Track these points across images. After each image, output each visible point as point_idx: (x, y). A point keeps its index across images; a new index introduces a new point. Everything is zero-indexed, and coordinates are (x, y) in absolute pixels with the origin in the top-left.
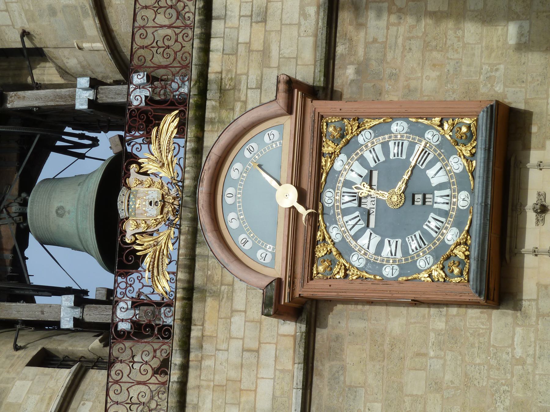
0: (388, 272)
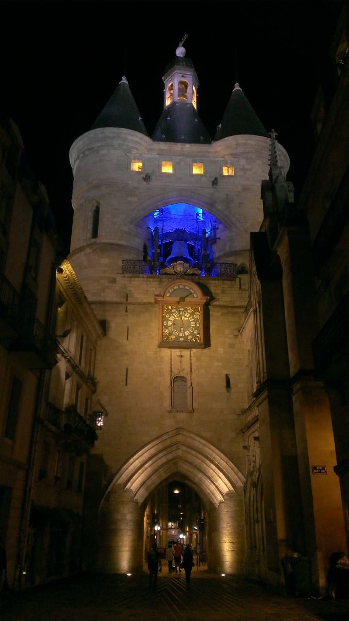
0: (165, 323)
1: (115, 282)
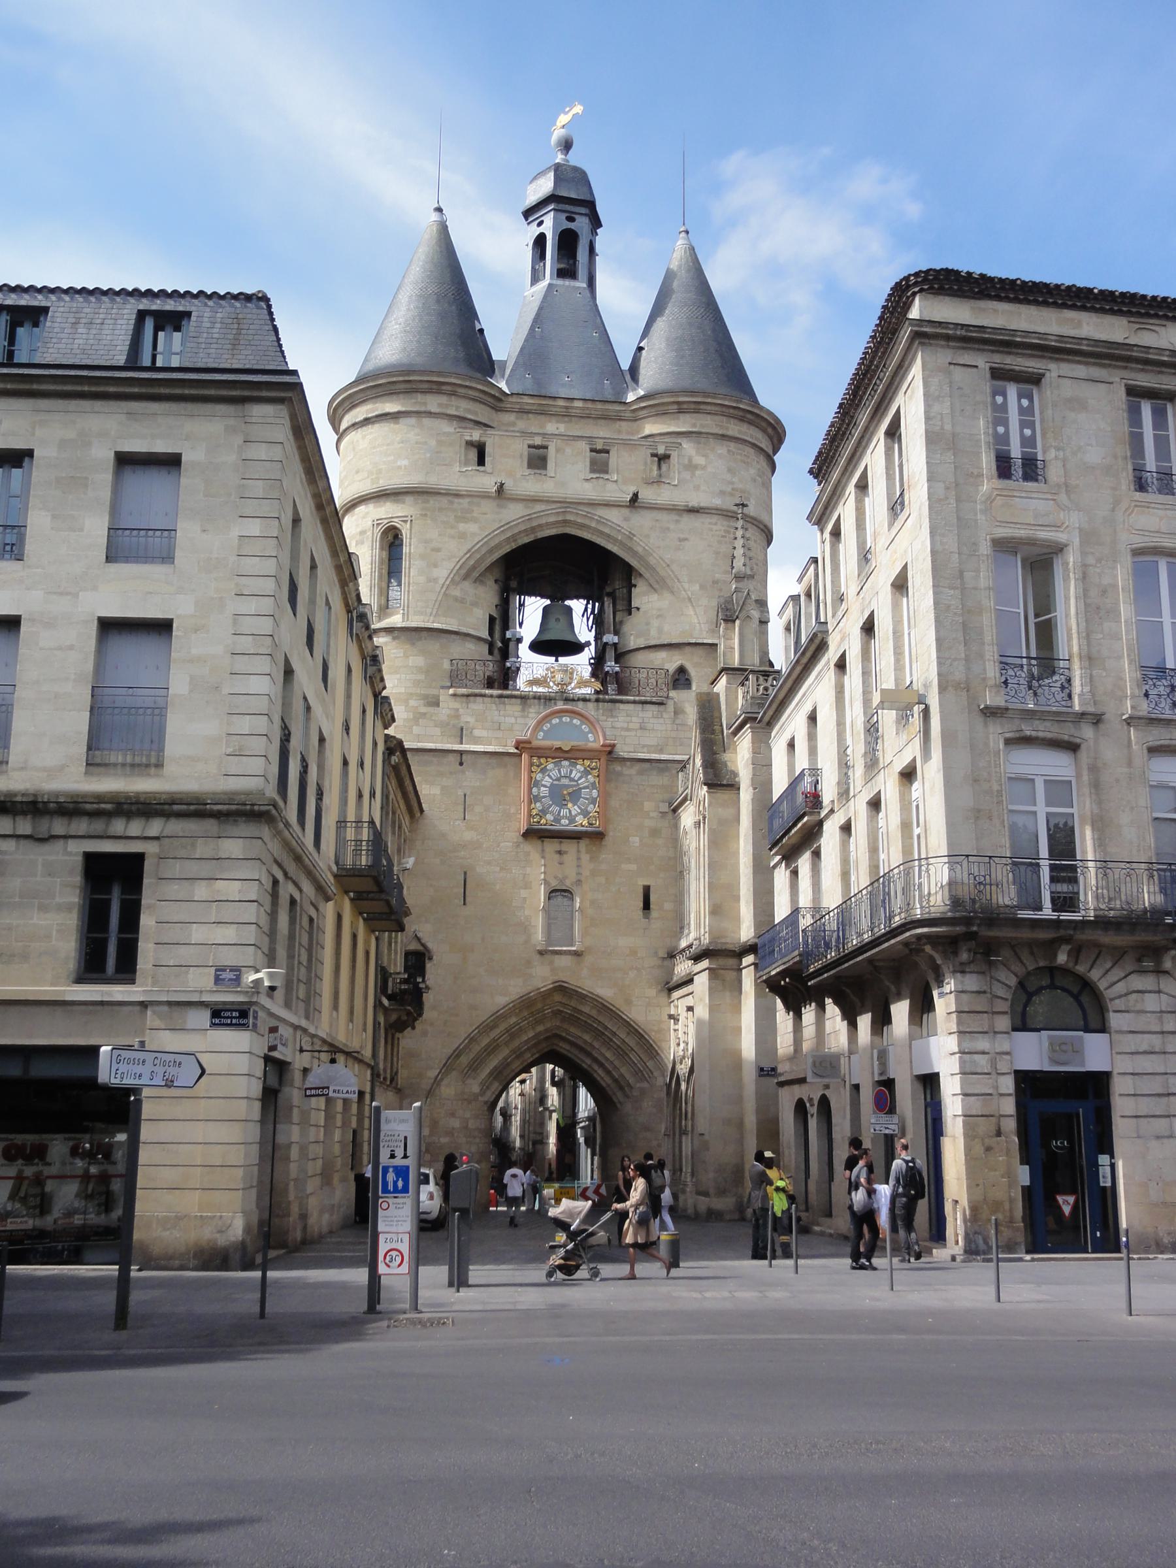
0: (535, 790)
1: (437, 704)
